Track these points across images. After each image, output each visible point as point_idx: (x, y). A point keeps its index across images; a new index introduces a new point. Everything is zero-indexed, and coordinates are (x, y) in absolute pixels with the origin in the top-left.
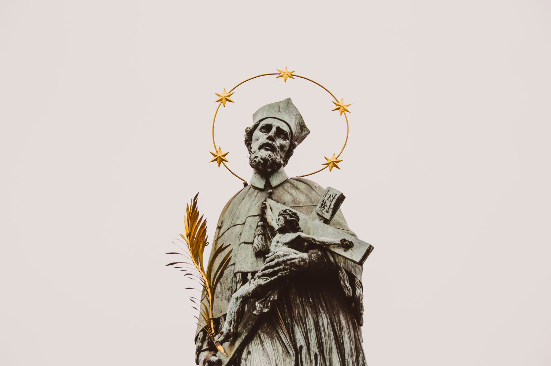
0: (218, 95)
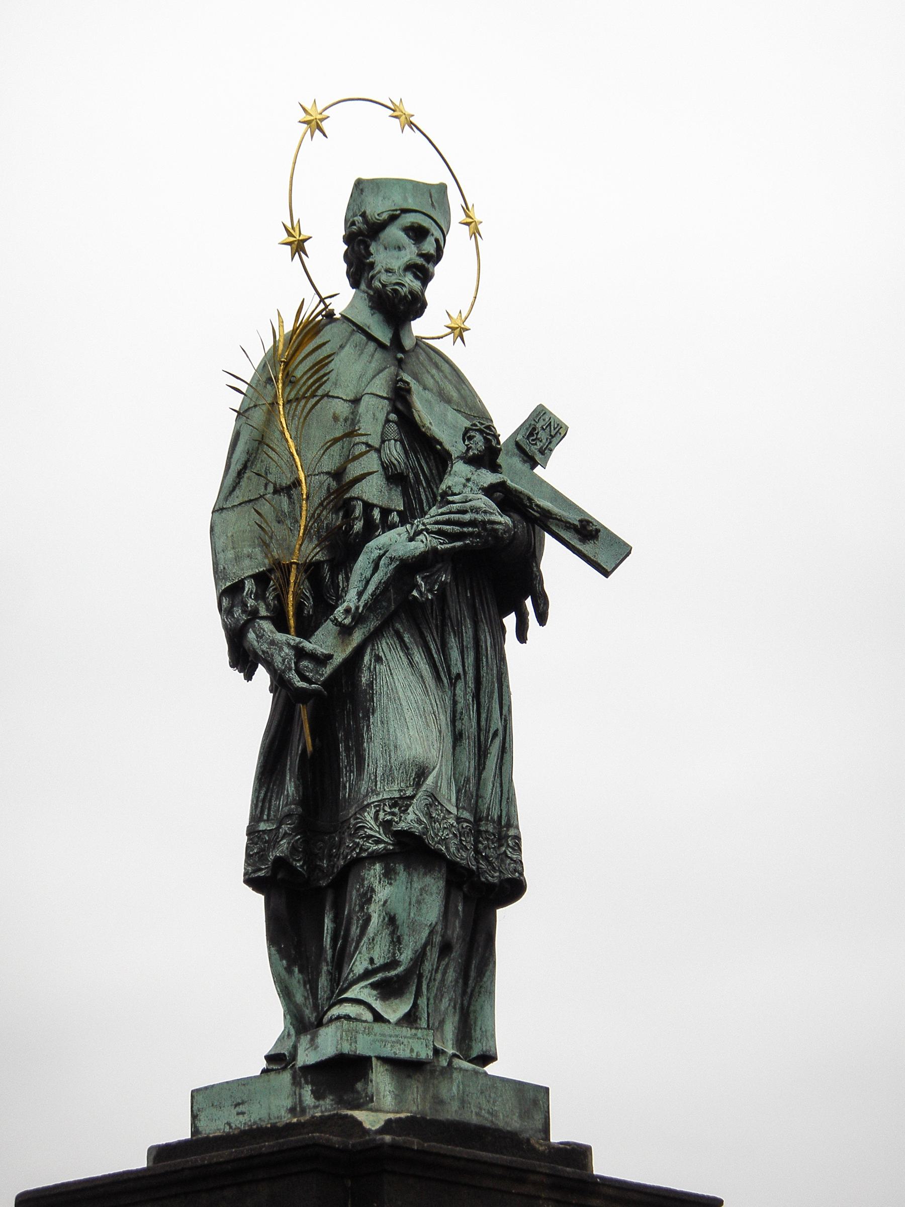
0: (304, 109)
